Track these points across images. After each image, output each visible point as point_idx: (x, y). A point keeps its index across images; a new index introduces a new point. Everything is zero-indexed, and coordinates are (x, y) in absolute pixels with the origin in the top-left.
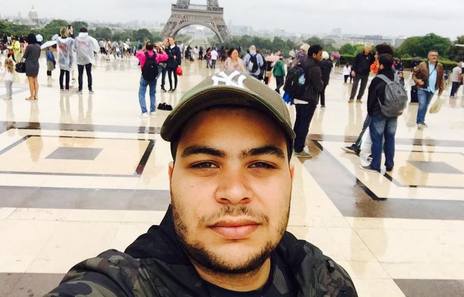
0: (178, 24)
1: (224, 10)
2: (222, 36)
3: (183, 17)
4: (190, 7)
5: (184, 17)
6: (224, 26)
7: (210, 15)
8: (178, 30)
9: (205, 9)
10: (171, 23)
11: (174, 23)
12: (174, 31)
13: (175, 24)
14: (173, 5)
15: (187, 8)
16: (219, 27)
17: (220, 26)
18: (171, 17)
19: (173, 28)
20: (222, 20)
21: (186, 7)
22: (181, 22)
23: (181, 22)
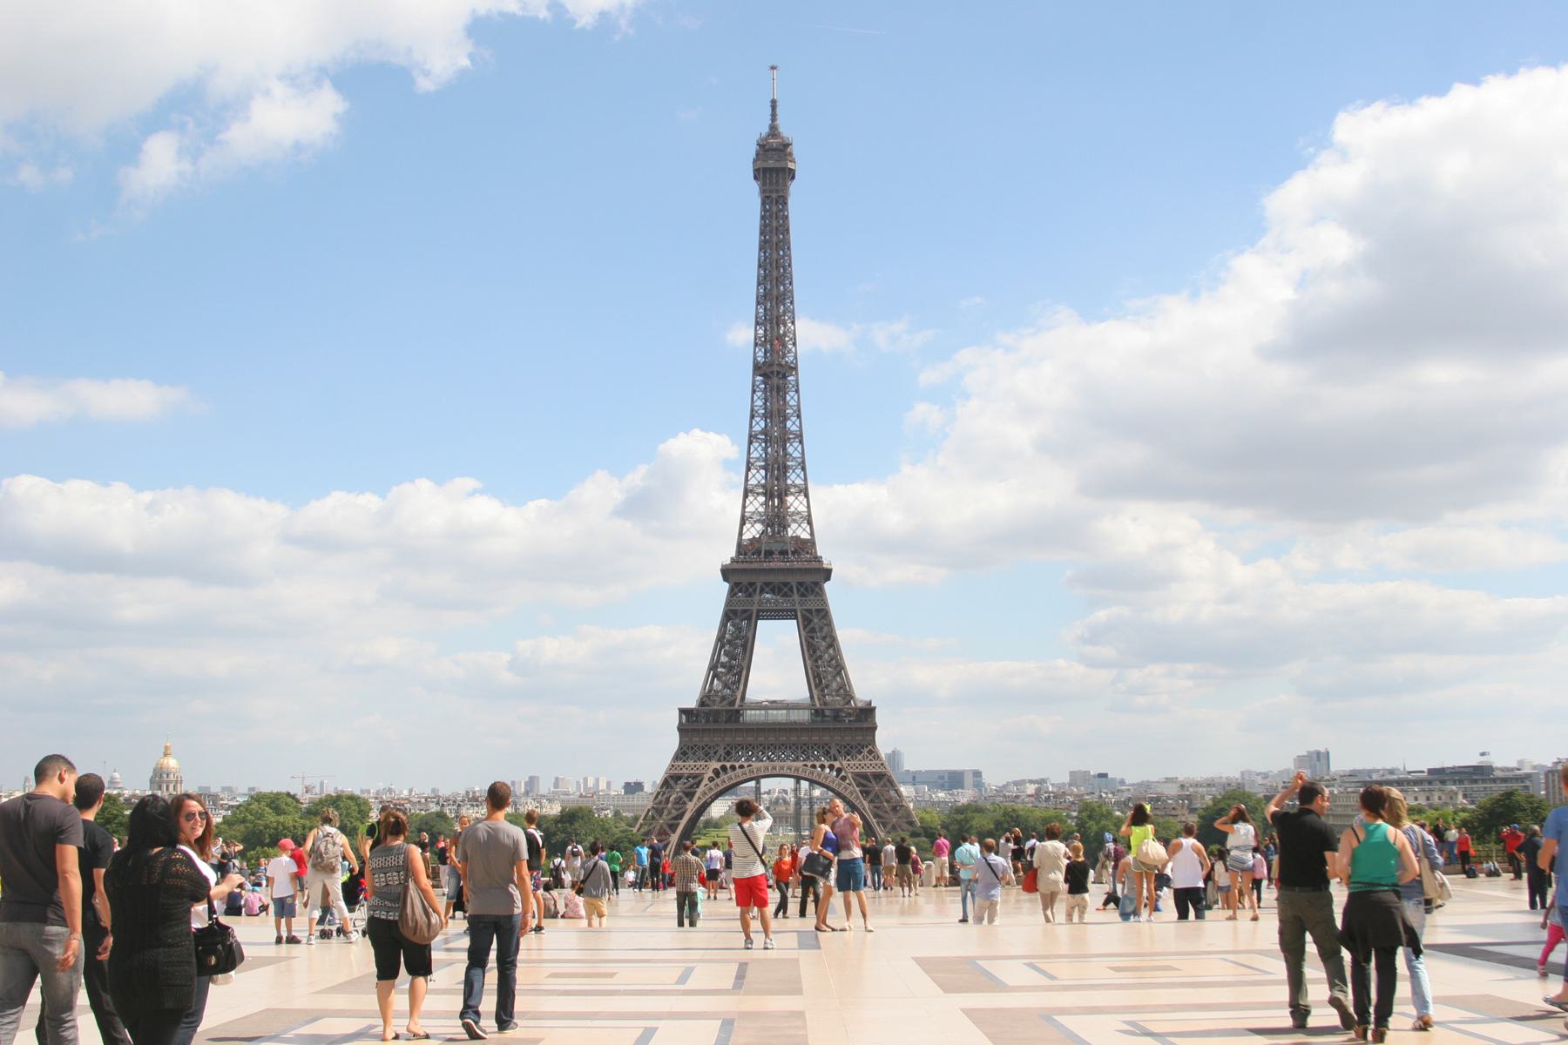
0: (706, 781)
1: (880, 718)
2: (876, 816)
3: (722, 752)
4: (751, 715)
5: (728, 753)
6: (879, 777)
7: (826, 738)
8: (705, 807)
9: (804, 716)
10: (677, 778)
11: (695, 777)
12: (691, 807)
13: (697, 779)
14: (682, 711)
15: (737, 721)
16: (863, 780)
17: (864, 776)
18: (676, 758)
19: (690, 795)
20: (870, 752)
21: (735, 715)
22: (717, 773)
23: (717, 773)
